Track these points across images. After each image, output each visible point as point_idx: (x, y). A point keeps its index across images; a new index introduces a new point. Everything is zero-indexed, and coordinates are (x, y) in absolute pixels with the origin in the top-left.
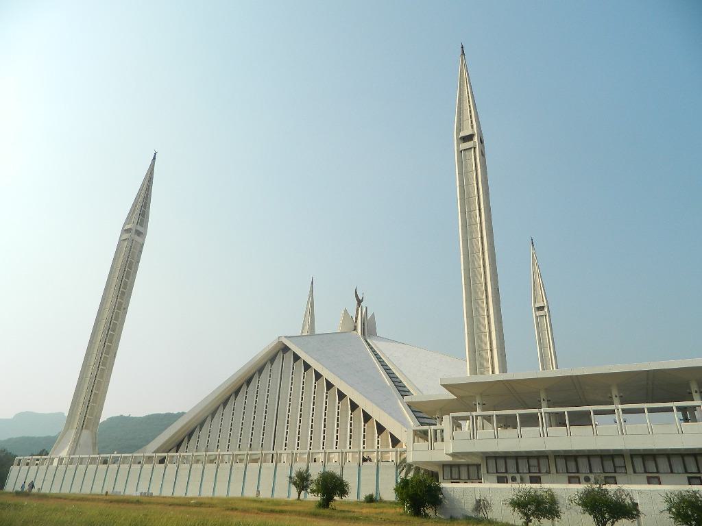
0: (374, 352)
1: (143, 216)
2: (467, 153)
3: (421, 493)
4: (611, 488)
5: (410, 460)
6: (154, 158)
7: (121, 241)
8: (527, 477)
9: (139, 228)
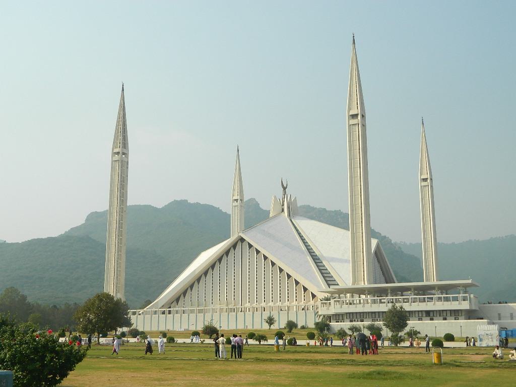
0: (297, 230)
1: (125, 141)
2: (353, 127)
3: (323, 327)
4: (376, 323)
5: (320, 313)
6: (123, 90)
7: (113, 162)
8: (359, 320)
9: (125, 151)
